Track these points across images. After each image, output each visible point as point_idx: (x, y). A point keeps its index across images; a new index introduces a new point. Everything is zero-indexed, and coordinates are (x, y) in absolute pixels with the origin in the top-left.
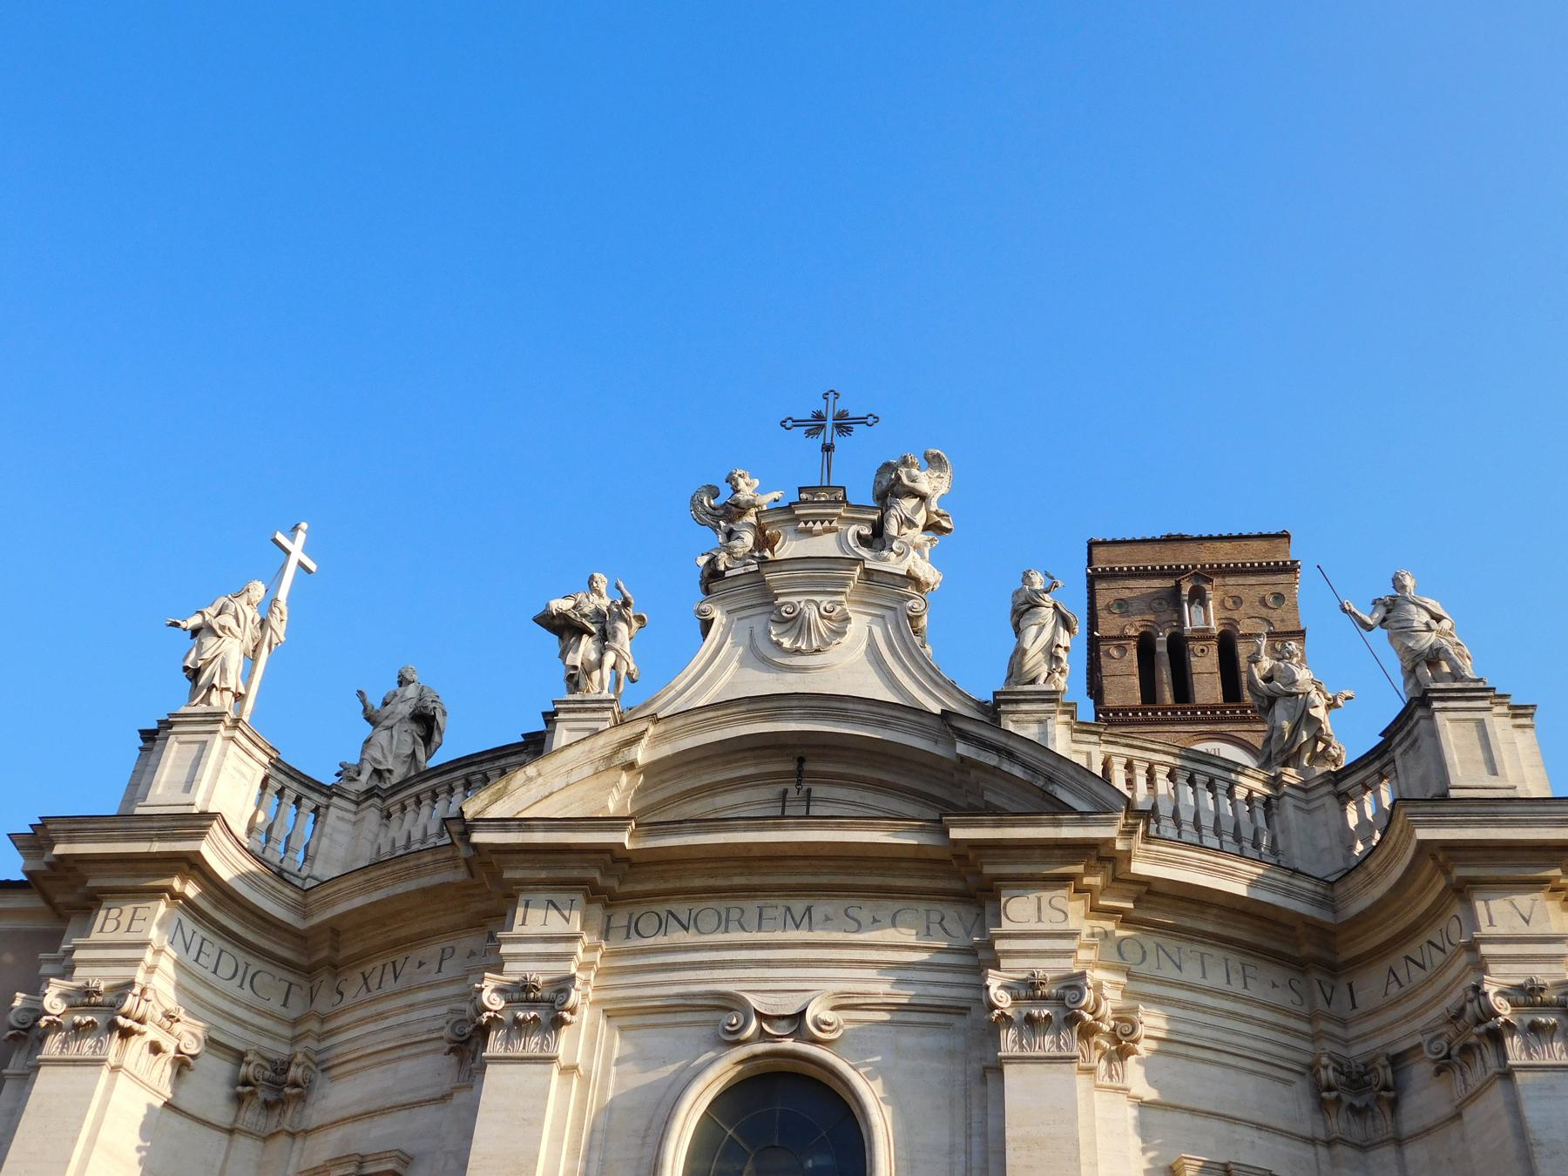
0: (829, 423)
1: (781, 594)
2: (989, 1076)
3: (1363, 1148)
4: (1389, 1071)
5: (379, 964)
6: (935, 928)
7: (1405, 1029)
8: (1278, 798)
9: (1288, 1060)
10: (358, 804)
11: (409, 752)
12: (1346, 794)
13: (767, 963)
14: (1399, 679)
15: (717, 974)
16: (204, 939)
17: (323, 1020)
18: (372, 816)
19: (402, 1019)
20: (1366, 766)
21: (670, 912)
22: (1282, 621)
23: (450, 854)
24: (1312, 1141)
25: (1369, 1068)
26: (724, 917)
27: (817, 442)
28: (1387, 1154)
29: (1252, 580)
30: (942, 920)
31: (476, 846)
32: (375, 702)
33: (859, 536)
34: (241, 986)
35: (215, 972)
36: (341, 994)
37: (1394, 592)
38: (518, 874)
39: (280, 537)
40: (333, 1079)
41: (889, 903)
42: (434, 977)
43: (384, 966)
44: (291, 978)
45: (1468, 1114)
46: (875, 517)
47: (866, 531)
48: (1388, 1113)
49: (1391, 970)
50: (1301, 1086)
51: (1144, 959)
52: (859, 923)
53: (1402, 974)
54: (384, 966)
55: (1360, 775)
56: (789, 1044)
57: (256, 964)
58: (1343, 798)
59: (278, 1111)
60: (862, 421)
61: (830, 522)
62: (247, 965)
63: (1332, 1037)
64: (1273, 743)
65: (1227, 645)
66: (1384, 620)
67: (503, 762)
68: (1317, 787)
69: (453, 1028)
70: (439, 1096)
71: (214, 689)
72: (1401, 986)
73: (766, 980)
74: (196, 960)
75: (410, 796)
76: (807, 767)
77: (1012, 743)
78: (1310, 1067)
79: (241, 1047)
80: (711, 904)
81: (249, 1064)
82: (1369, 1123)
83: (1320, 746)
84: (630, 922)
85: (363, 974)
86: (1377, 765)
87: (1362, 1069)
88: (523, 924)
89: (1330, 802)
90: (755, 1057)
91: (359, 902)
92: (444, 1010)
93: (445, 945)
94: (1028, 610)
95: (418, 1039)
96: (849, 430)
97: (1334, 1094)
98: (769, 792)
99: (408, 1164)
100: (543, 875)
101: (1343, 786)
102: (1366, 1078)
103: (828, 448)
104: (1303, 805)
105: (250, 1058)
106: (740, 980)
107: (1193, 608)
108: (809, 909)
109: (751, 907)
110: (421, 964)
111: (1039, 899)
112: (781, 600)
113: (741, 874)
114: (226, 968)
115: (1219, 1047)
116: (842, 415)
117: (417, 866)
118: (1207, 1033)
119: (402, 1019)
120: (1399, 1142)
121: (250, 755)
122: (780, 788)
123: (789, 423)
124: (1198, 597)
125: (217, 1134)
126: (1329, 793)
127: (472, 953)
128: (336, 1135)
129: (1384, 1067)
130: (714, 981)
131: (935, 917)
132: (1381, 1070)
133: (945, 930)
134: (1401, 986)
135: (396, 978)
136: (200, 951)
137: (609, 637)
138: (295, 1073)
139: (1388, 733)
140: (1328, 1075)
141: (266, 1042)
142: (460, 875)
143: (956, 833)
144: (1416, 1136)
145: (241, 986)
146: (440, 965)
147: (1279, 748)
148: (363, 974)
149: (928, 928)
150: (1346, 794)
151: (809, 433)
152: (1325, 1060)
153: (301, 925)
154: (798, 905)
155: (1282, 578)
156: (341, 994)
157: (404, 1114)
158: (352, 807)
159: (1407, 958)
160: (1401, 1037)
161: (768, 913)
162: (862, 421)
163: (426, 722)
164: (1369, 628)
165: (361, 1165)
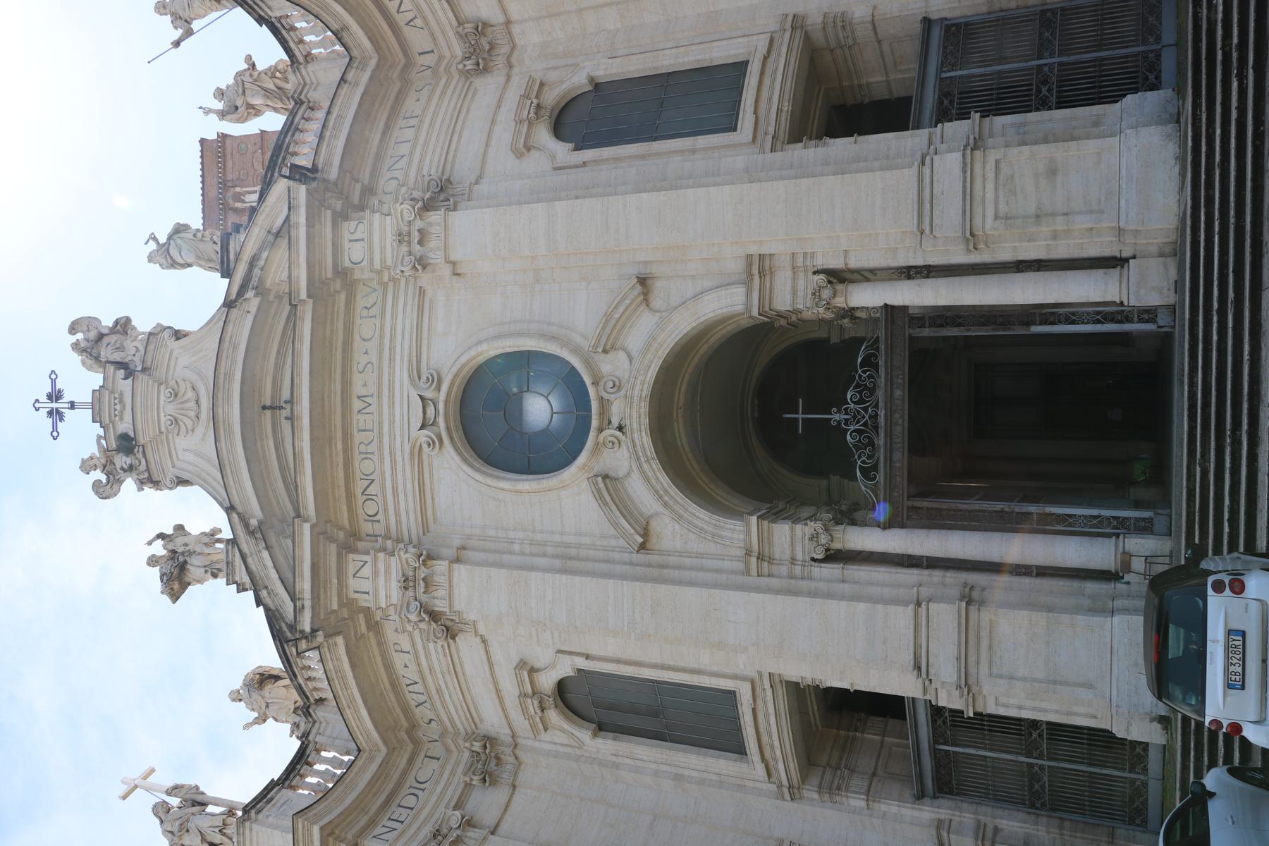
0: (55, 405)
1: (160, 430)
2: (459, 271)
4: (466, 25)
5: (409, 696)
6: (372, 312)
7: (441, 14)
8: (309, 102)
9: (462, 91)
10: (315, 722)
11: (284, 689)
12: (306, 57)
13: (392, 423)
16: (389, 819)
17: (444, 733)
19: (439, 675)
20: (286, 42)
21: (363, 493)
22: (255, 144)
23: (326, 650)
24: (509, 77)
25: (463, 37)
26: (365, 456)
27: (68, 414)
28: (516, 29)
30: (366, 308)
31: (314, 631)
33: (126, 378)
34: (423, 790)
35: (412, 809)
36: (431, 720)
38: (335, 599)
40: (481, 721)
41: (356, 345)
43: (410, 692)
44: (422, 756)
46: (112, 367)
47: (121, 373)
48: (491, 29)
49: (407, 24)
50: (479, 82)
51: (397, 178)
52: (368, 363)
53: (409, 16)
54: (410, 692)
55: (292, 45)
56: (441, 407)
57: (411, 781)
58: (308, 57)
59: (503, 756)
60: (53, 382)
61: (115, 398)
62: (411, 787)
63: (449, 65)
64: (276, 106)
66: (186, 21)
68: (302, 77)
69: (438, 638)
70: (483, 645)
71: (224, 831)
72: (416, 17)
73: (402, 425)
74: (402, 822)
75: (306, 685)
76: (268, 403)
78: (467, 78)
80: (357, 466)
81: (472, 779)
82: (499, 42)
83: (278, 74)
84: (369, 521)
85: (417, 706)
86: (284, 32)
87: (467, 45)
88: (368, 593)
89: (310, 67)
90: (448, 428)
92: (431, 645)
93: (393, 650)
94: (171, 258)
95: (450, 663)
96: (60, 391)
97: (480, 61)
99: (525, 663)
101: (301, 59)
102: (473, 42)
103: (72, 405)
104: (313, 88)
105: (467, 779)
106: (402, 442)
107: (247, 200)
108: (359, 397)
109: (358, 437)
110: (406, 666)
111: (350, 241)
112: (163, 429)
113: (336, 444)
114: (410, 801)
115: (451, 131)
116: (50, 397)
117: (336, 673)
118: (442, 138)
119: (439, 675)
120: (508, 23)
121: (272, 799)
122: (284, 421)
123: (55, 434)
125: (516, 797)
126: (305, 68)
129: (464, 28)
130: (403, 459)
131: (365, 312)
132: (466, 30)
133: (372, 306)
134: (416, 17)
135: (416, 683)
136: (397, 821)
137: (187, 548)
138: (477, 746)
140: (470, 65)
142: (340, 640)
144: (504, 10)
145: (423, 790)
146: (405, 652)
147: (278, 102)
148: (417, 706)
149: (371, 317)
150: (306, 57)
151: (61, 420)
152: (460, 66)
153: (384, 750)
154: (357, 405)
155: (228, 142)
156: (431, 720)
157: (496, 668)
158: (317, 725)
159: (398, 12)
161: (362, 426)
162: (53, 382)
164: (189, 33)
165: (526, 695)
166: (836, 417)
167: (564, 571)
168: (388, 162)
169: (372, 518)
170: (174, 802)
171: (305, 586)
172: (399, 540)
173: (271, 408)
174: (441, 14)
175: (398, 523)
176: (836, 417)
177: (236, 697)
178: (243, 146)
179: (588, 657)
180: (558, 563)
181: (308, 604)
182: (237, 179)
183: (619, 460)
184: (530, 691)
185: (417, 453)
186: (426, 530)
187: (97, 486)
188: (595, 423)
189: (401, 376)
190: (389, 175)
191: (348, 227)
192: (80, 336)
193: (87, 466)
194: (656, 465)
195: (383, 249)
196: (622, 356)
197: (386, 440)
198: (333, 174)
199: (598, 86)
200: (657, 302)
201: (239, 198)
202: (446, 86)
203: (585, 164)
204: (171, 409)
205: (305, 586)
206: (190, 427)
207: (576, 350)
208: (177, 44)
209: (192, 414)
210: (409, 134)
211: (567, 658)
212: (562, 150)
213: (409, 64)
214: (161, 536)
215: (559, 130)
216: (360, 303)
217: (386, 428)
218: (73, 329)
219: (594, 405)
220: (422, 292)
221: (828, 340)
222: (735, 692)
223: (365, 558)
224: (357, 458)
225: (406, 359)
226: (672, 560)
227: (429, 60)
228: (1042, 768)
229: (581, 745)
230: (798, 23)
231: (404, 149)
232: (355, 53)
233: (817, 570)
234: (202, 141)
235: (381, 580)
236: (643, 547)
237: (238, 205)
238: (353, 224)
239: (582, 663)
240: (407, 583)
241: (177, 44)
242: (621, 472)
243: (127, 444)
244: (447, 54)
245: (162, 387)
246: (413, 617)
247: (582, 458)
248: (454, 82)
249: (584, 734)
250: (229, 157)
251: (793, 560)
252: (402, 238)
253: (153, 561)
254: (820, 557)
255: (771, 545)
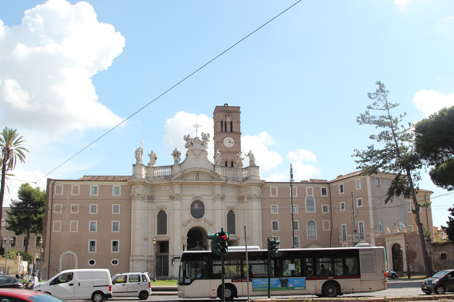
0: (197, 126)
3: (240, 203)
5: (159, 187)
6: (209, 188)
7: (245, 194)
14: (249, 162)
15: (192, 192)
17: (154, 192)
18: (153, 169)
28: (242, 203)
29: (235, 114)
32: (149, 154)
33: (202, 144)
37: (250, 152)
39: (141, 141)
42: (165, 190)
45: (249, 202)
55: (245, 169)
58: (243, 171)
65: (231, 123)
67: (168, 167)
76: (198, 172)
77: (217, 173)
79: (147, 195)
89: (242, 171)
91: (158, 183)
98: (196, 174)
100: (177, 184)
101: (243, 169)
103: (197, 130)
109: (194, 186)
122: (196, 174)
124: (229, 116)
127: (169, 188)
128: (158, 203)
138: (153, 197)
139: (247, 168)
140: (239, 198)
141: (149, 194)
143: (212, 182)
144: (245, 202)
154: (198, 186)
155: (239, 113)
158: (150, 168)
160: (245, 194)
161: (196, 187)
162: (200, 126)
163: (156, 158)
164: (247, 156)
165: (163, 207)
166: (198, 246)
167: (180, 215)
168: (228, 187)
169: (184, 187)
170: (141, 150)
171: (177, 181)
172: (182, 192)
173: (198, 173)
174: (245, 194)
175: (184, 192)
176: (198, 246)
177: (152, 152)
178: (238, 117)
179: (169, 216)
180: (181, 214)
181: (174, 181)
182: (232, 116)
183: (193, 222)
184: (163, 207)
185: (193, 195)
186: (183, 195)
187: (186, 136)
188: (197, 219)
189: (202, 193)
190: (226, 188)
191: (220, 186)
192: (207, 134)
193: (189, 136)
194: (192, 227)
195: (217, 191)
196: (204, 222)
197: (194, 191)
198: (226, 183)
199: (234, 215)
200: (210, 226)
201: (229, 116)
202: (237, 194)
203: (225, 216)
204: (197, 155)
205: (177, 181)
206: (195, 157)
207: (205, 217)
208: (245, 155)
209: (197, 158)
210: (231, 189)
211: (168, 213)
212: (227, 213)
213: (240, 187)
214: (181, 154)
215: (230, 211)
216: (211, 186)
217: (196, 191)
218: (208, 134)
219: (199, 219)
220: (212, 195)
221: (203, 239)
222: (166, 234)
223: (180, 187)
224: (192, 186)
225: (204, 194)
226: (182, 228)
227: (240, 190)
228: (162, 266)
229: (156, 212)
230: (238, 239)
231: (229, 189)
232: (241, 183)
233: (183, 245)
234: (239, 107)
235: (177, 190)
236: (183, 225)
237: (227, 116)
238: (220, 187)
239: (168, 215)
240: (177, 195)
241: (245, 155)
242: (192, 222)
243: (192, 144)
244: (241, 193)
245: (200, 153)
246: (174, 196)
247: (193, 218)
248: (237, 195)
249: (157, 213)
250: (237, 114)
251: (183, 242)
252: (218, 195)
253: (176, 149)
254: (184, 245)
255: (185, 239)
